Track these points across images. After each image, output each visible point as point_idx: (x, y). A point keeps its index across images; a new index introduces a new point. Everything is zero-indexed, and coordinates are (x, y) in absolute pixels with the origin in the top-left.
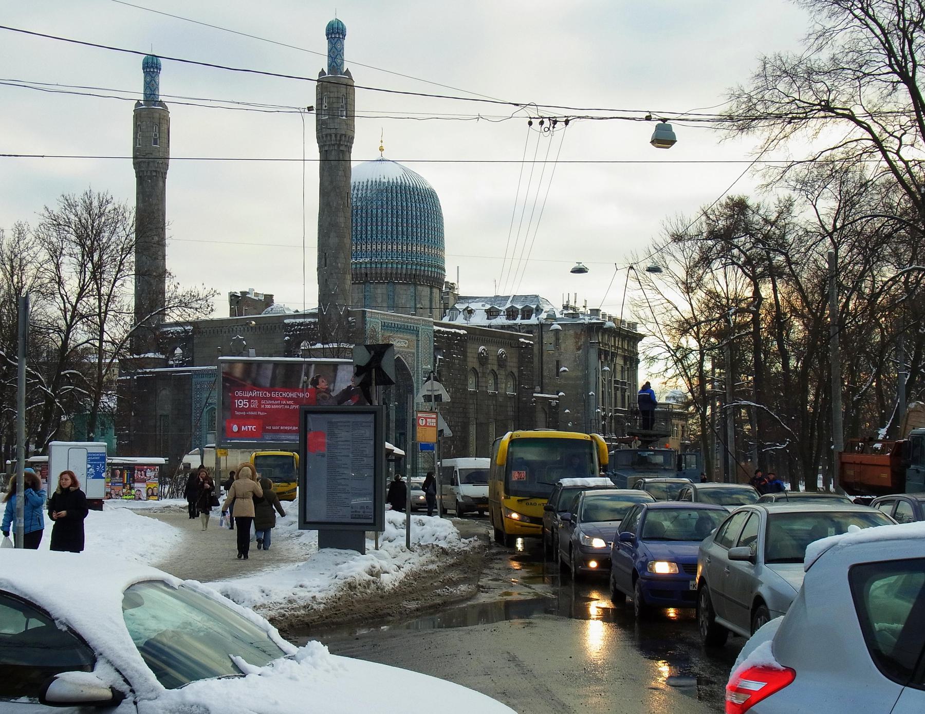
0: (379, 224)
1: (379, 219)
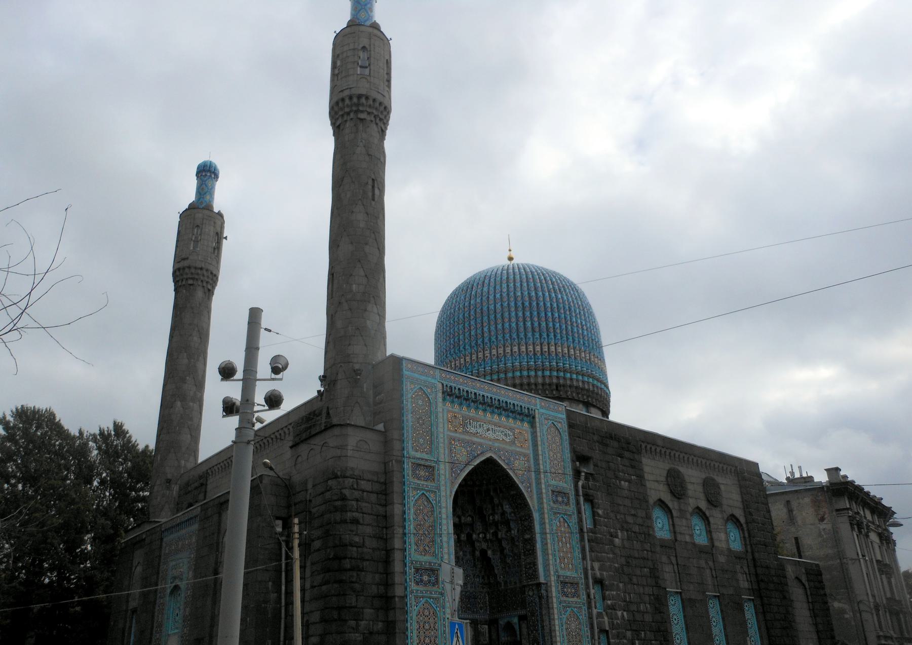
0: (499, 321)
1: (499, 316)
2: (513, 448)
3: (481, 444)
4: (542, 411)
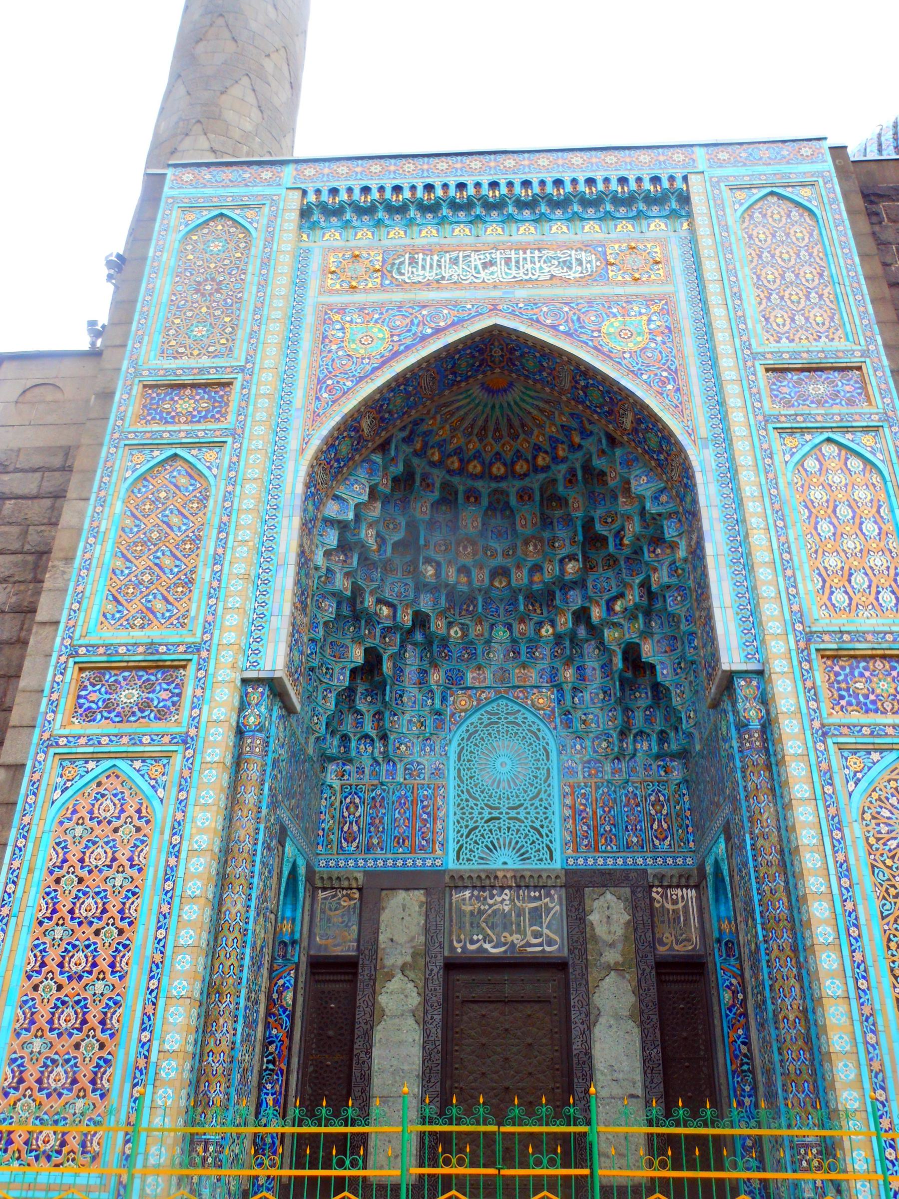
2: (595, 290)
3: (456, 303)
4: (719, 172)
